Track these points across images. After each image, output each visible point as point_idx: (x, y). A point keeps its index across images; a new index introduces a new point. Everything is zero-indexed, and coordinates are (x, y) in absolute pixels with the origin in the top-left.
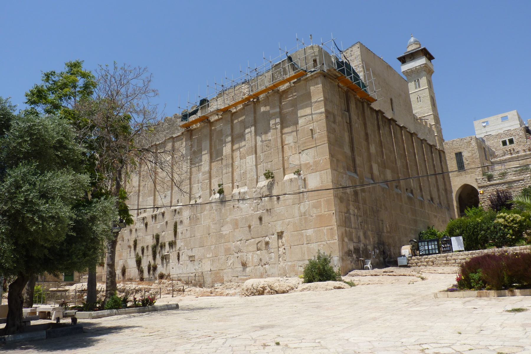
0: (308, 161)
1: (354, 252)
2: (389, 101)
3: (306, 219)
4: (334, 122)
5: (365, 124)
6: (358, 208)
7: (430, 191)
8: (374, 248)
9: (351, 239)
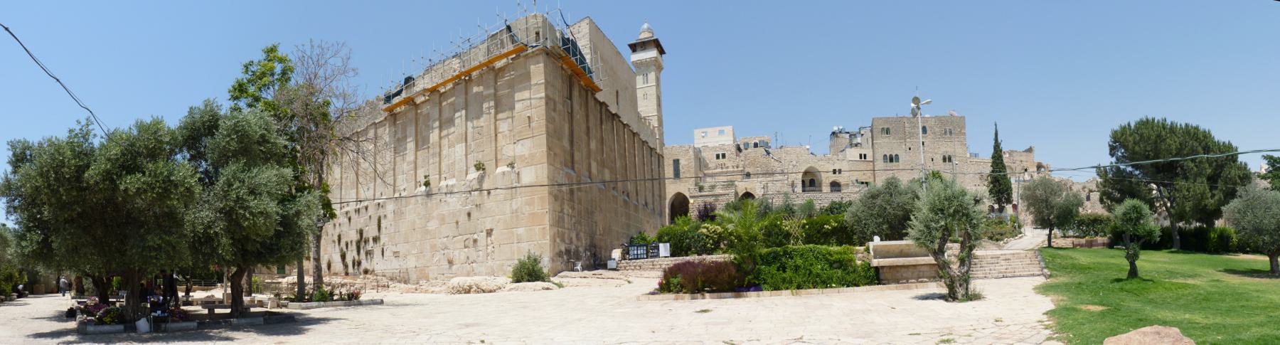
1: (566, 254)
3: (517, 216)
6: (573, 209)
7: (645, 196)
8: (586, 250)
9: (563, 240)
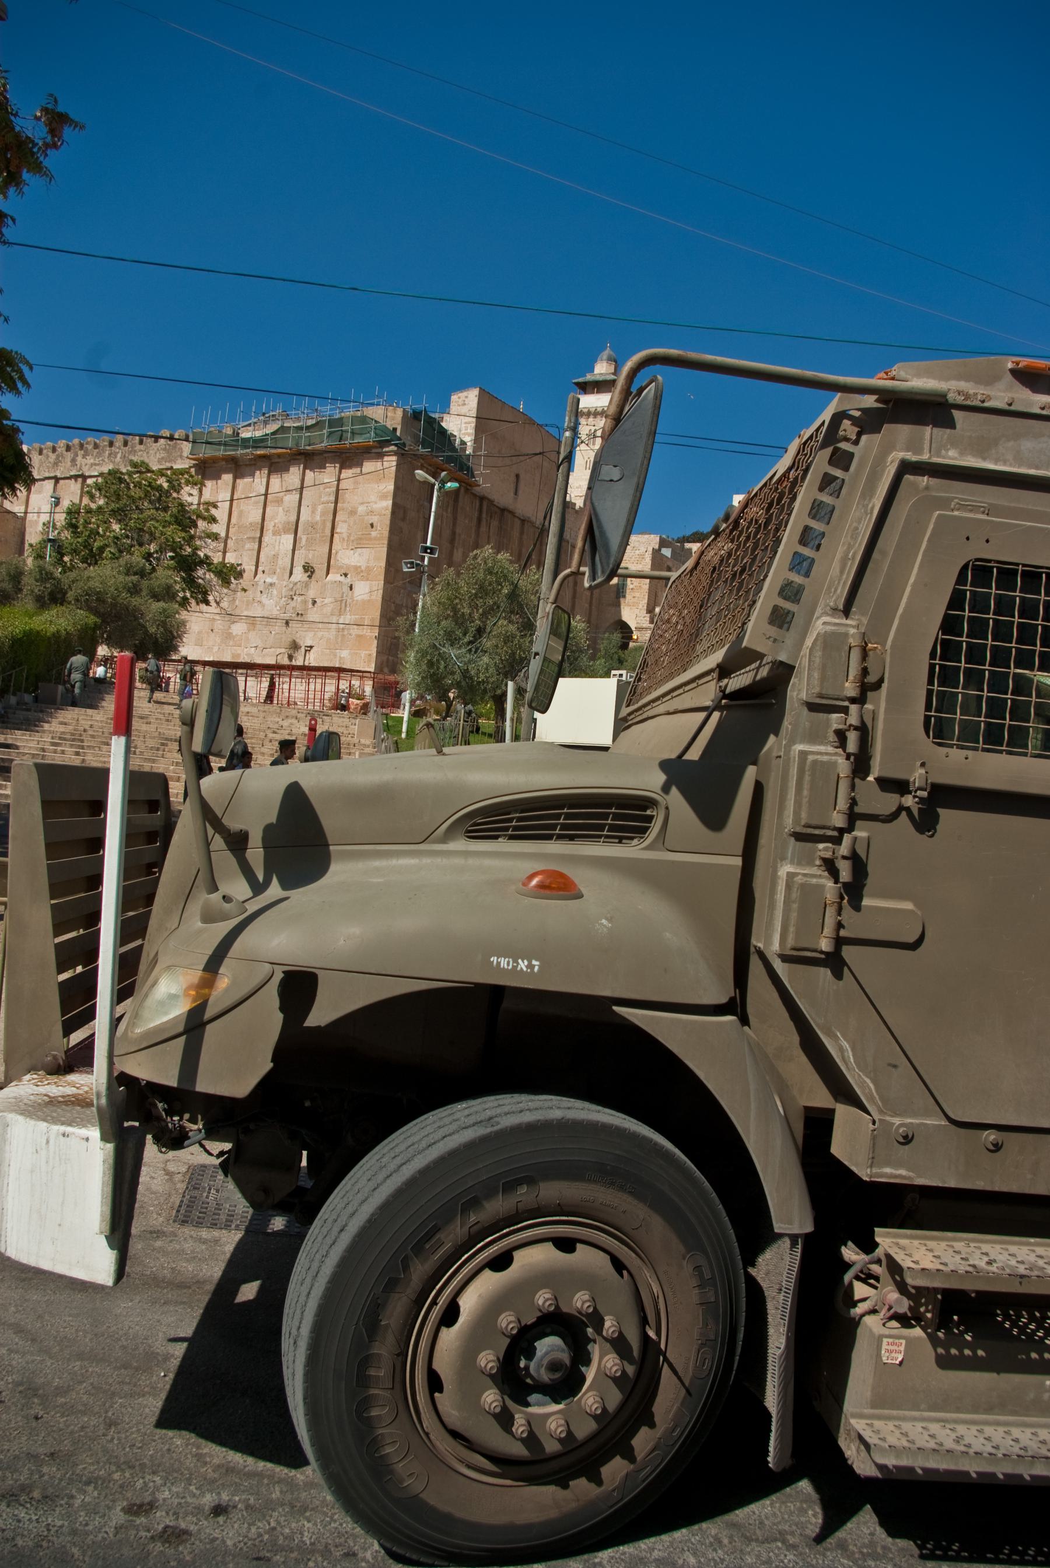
0: (358, 564)
2: (513, 478)
4: (403, 519)
5: (455, 519)
